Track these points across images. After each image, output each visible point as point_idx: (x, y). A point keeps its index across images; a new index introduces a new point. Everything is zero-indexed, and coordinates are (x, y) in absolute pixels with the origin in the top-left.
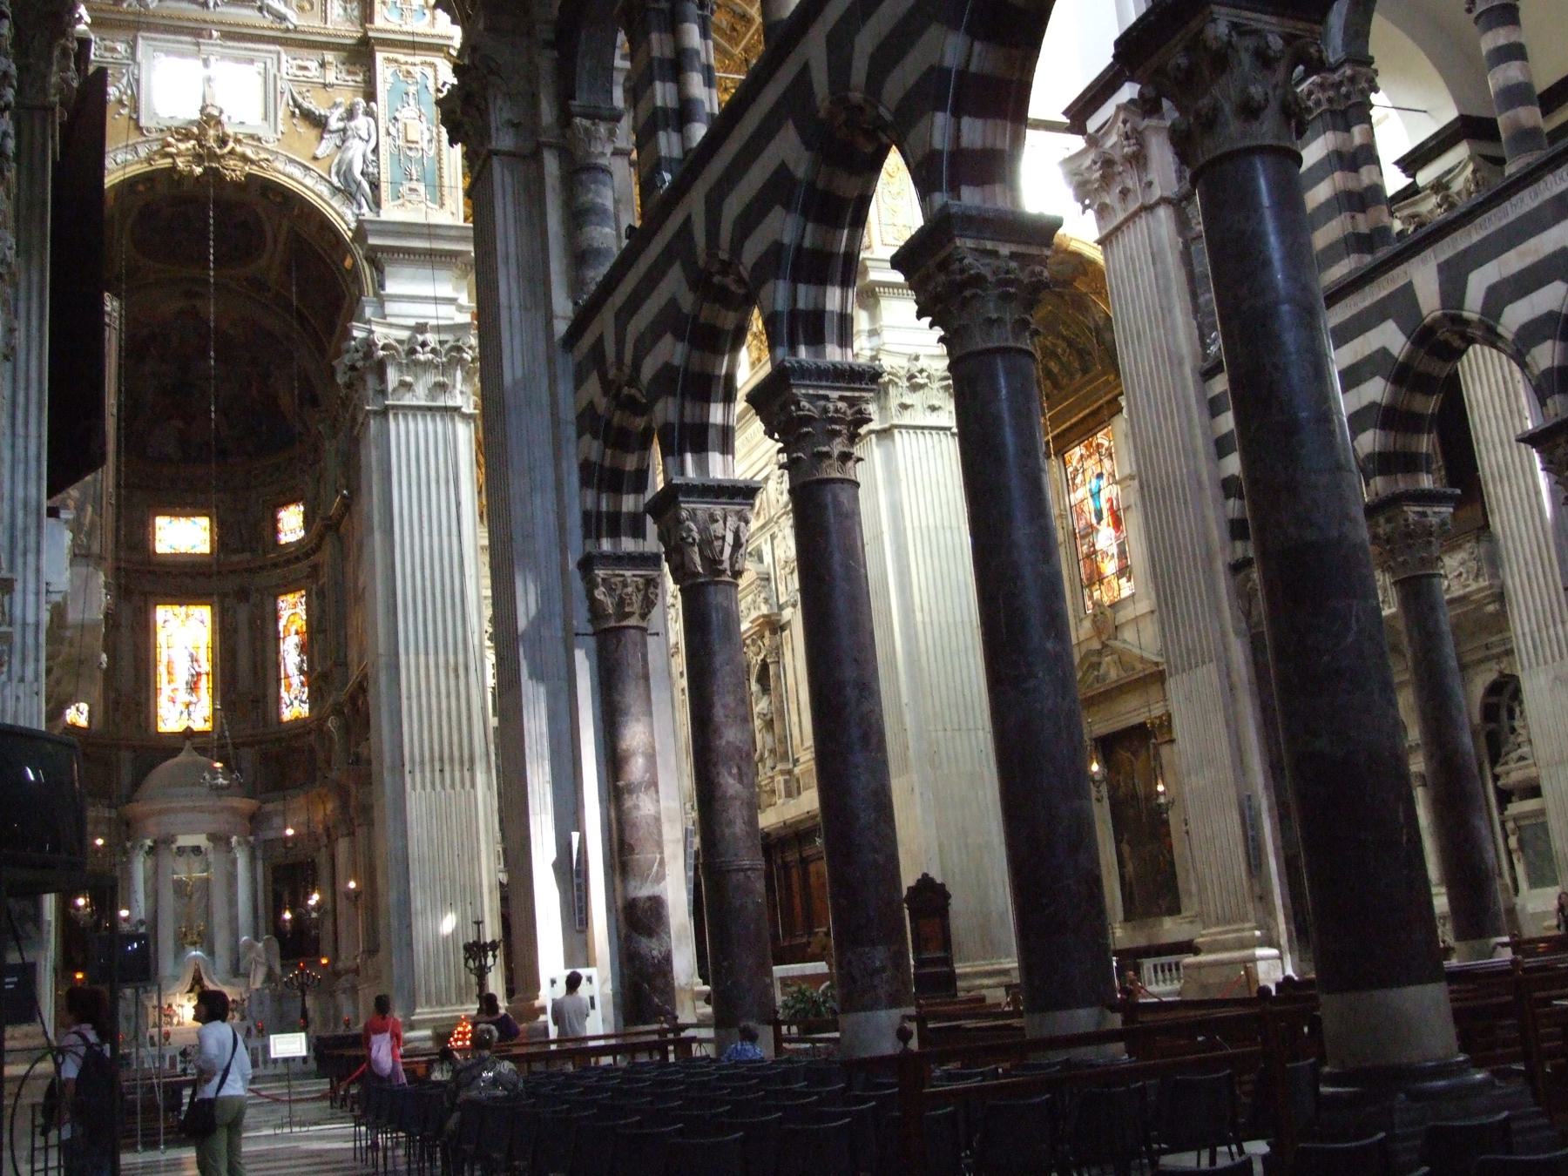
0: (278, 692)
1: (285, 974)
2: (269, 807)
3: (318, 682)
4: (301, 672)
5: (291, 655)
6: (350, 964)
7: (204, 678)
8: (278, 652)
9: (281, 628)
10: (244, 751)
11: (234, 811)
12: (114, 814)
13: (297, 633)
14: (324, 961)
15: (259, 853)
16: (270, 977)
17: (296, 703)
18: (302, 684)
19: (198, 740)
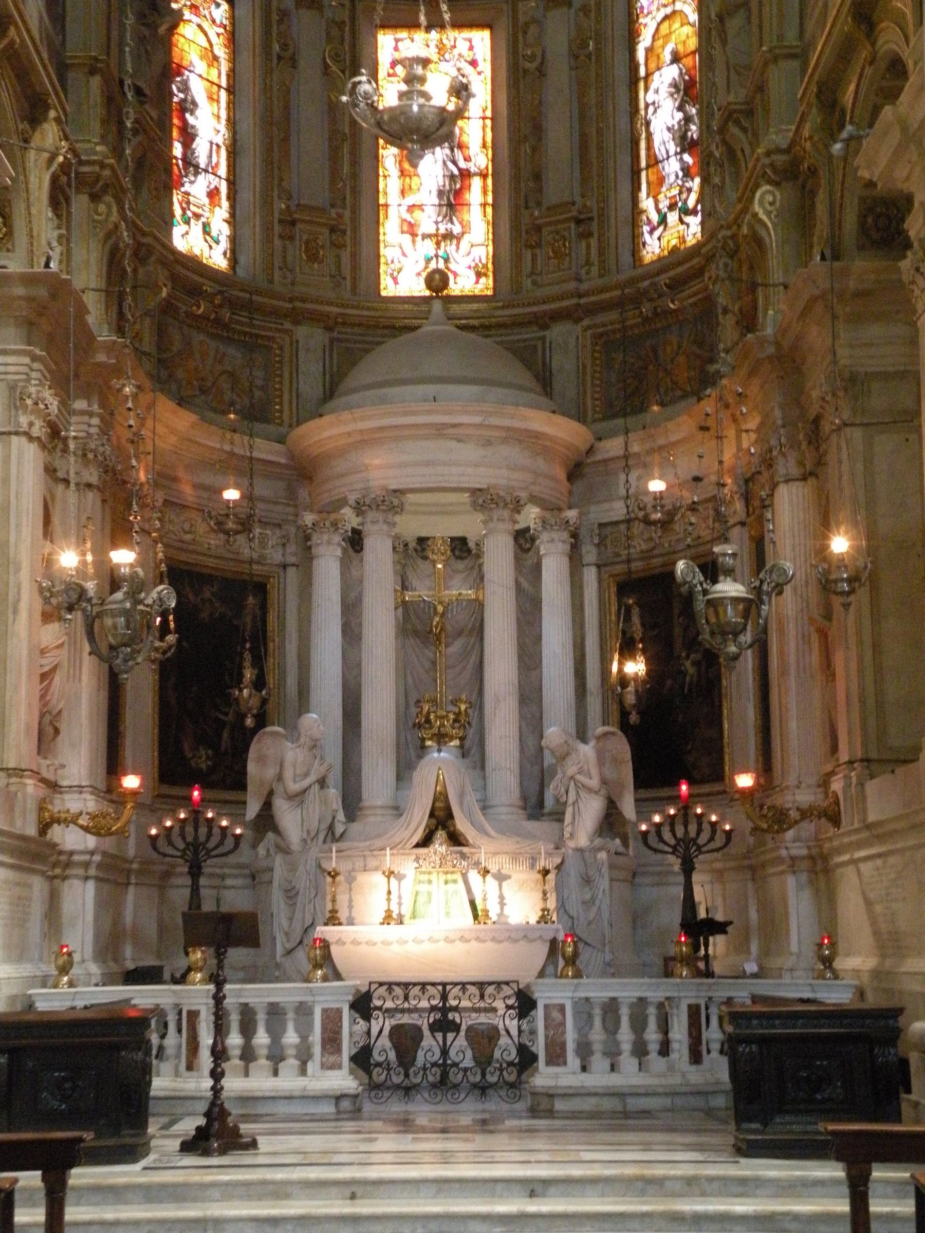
0: (635, 201)
1: (643, 815)
2: (613, 447)
3: (717, 147)
4: (685, 144)
5: (662, 114)
6: (805, 797)
7: (476, 183)
8: (636, 110)
9: (641, 55)
10: (558, 332)
11: (530, 440)
12: (265, 450)
13: (676, 58)
14: (745, 781)
15: (590, 554)
16: (611, 821)
17: (673, 217)
18: (687, 172)
19: (456, 309)
